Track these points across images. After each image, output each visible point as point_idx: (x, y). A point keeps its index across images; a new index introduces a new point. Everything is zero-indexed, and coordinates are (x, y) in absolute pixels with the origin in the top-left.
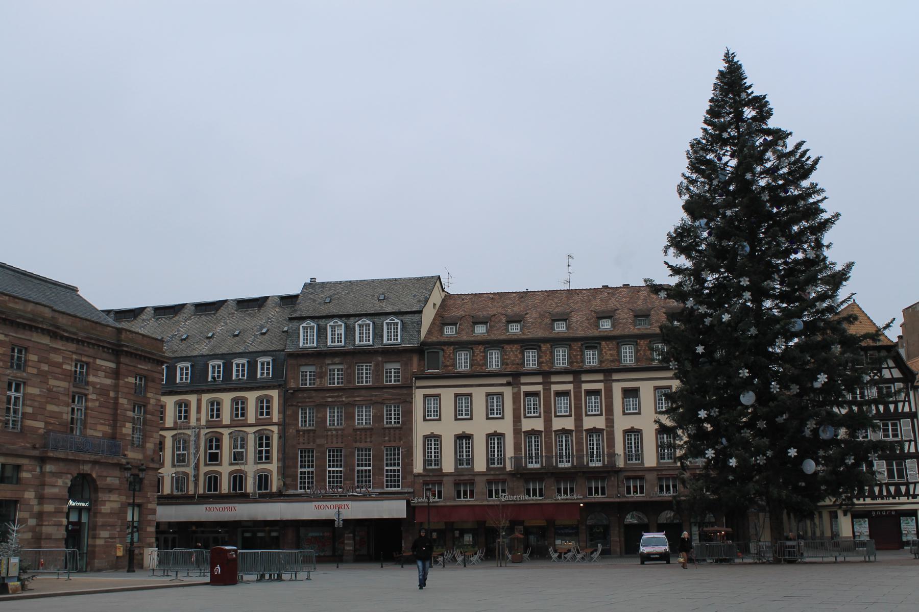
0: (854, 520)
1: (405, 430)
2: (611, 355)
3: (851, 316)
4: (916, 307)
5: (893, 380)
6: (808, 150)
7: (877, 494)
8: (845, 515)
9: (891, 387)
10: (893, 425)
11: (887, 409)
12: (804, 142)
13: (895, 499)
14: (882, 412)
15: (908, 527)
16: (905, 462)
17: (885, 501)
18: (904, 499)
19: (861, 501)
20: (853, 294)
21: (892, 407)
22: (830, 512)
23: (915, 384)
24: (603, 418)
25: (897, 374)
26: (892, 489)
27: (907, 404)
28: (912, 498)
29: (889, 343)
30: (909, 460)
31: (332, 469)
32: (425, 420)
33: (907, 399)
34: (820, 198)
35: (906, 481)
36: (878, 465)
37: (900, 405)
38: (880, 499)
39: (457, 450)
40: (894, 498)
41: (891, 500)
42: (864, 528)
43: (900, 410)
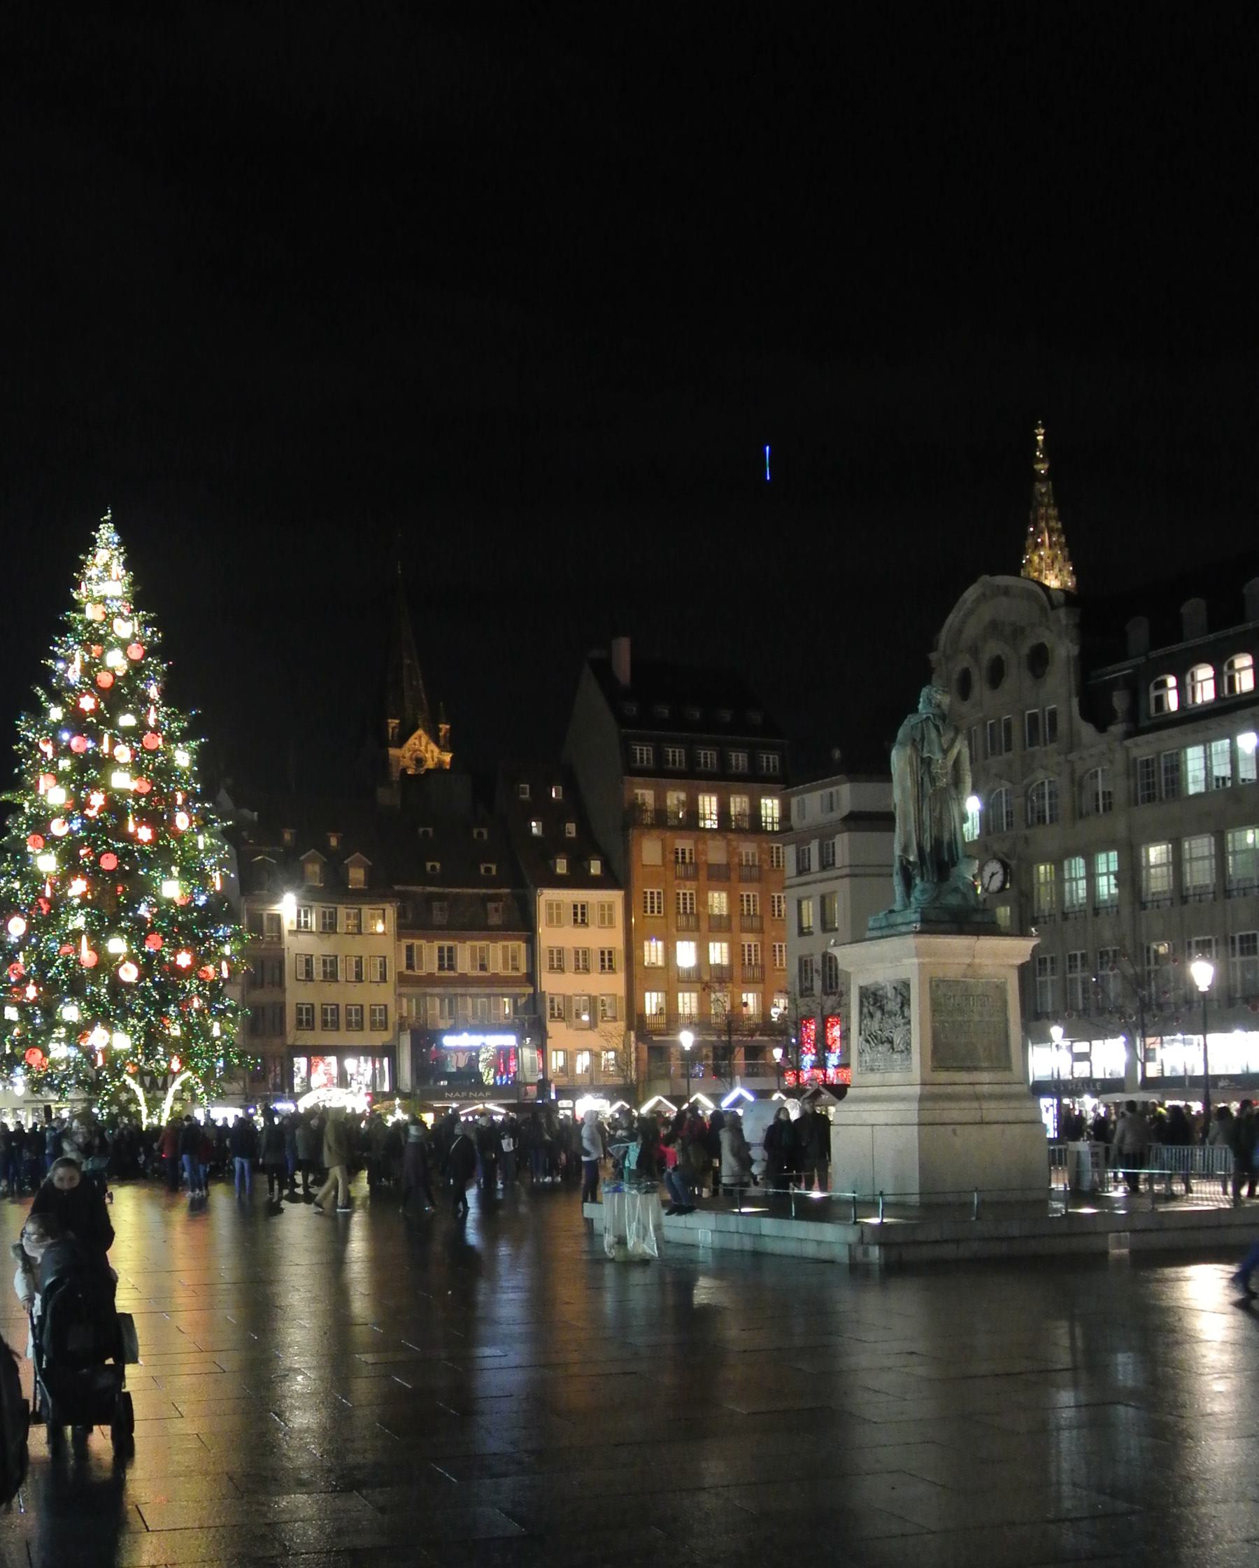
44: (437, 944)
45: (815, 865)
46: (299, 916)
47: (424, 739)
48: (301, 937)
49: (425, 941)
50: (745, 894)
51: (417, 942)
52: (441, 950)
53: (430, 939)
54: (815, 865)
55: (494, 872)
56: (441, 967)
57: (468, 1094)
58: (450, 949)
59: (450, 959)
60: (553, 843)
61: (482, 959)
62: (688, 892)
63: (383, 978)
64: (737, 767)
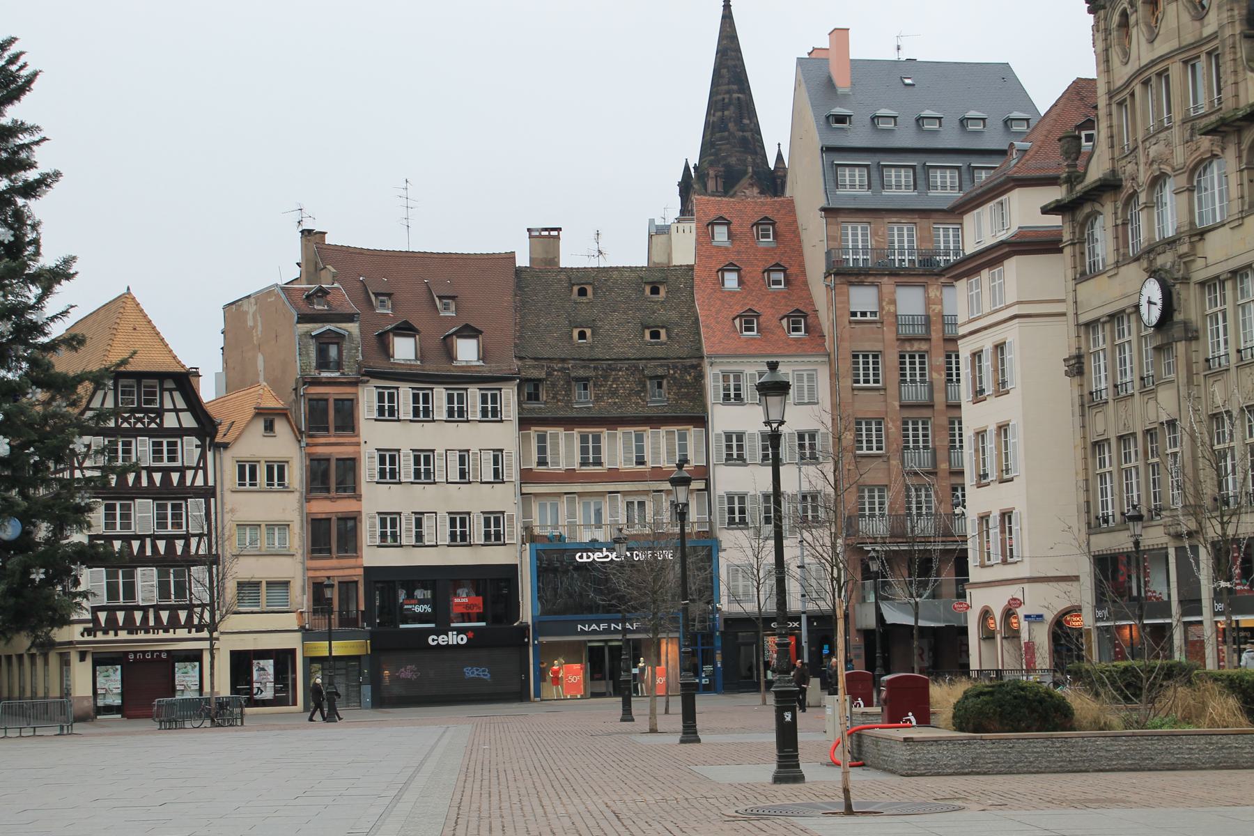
0: (98, 668)
3: (74, 338)
4: (241, 304)
5: (181, 432)
6: (22, 53)
7: (138, 624)
8: (82, 657)
9: (176, 442)
10: (174, 507)
11: (166, 479)
12: (16, 39)
13: (168, 632)
14: (158, 485)
15: (187, 679)
16: (189, 571)
17: (151, 636)
18: (182, 633)
19: (111, 636)
20: (72, 307)
21: (175, 477)
22: (61, 654)
23: (218, 439)
25: (188, 421)
26: (165, 615)
27: (200, 472)
28: (197, 632)
29: (179, 369)
30: (195, 568)
33: (201, 465)
34: (37, 137)
35: (188, 602)
36: (144, 574)
37: (189, 474)
38: (143, 632)
40: (166, 631)
41: (162, 635)
42: (112, 681)
43: (188, 483)
44: (576, 433)
49: (562, 429)
51: (550, 431)
52: (584, 439)
56: (584, 463)
57: (610, 626)
59: (597, 450)
63: (498, 476)
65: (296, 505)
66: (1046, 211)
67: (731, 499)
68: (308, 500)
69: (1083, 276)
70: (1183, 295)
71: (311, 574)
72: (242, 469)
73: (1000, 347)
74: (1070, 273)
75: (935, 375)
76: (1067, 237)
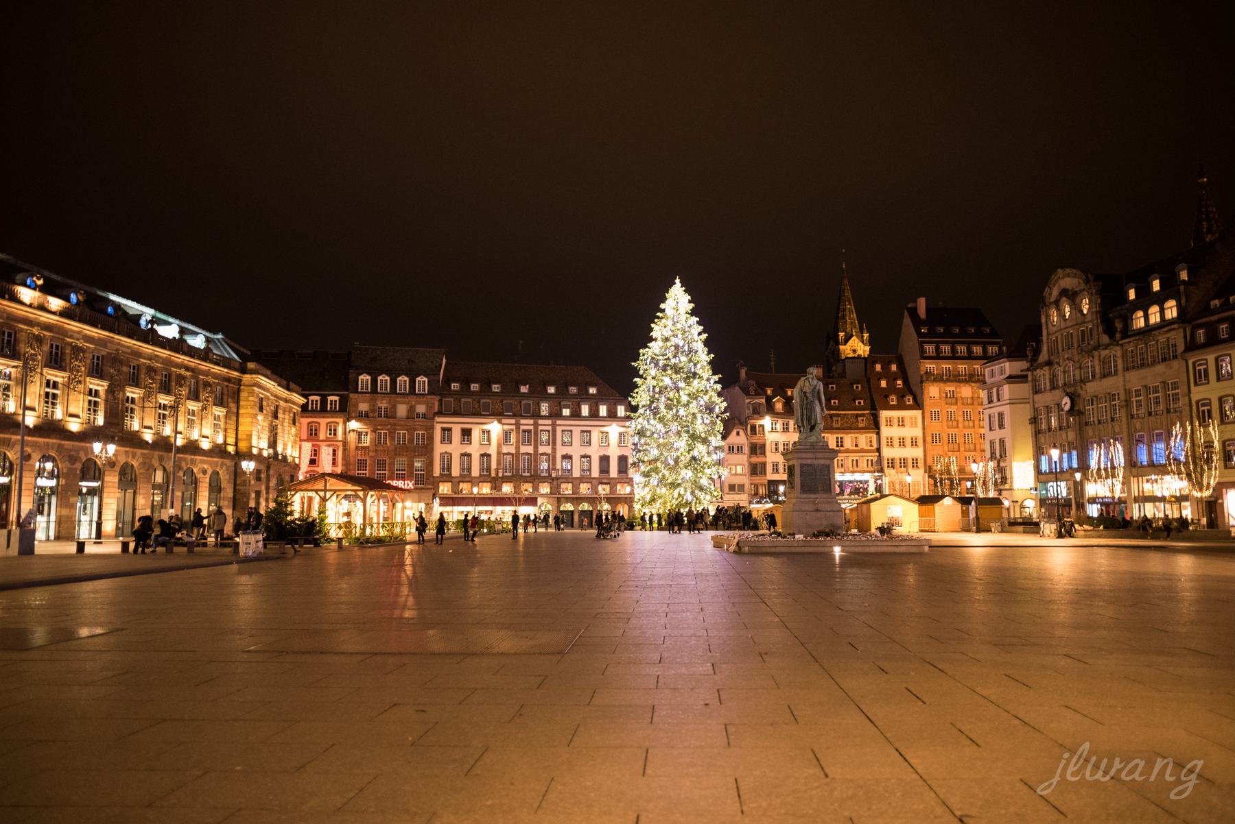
1: (427, 450)
2: (556, 410)
24: (550, 447)
31: (379, 472)
32: (441, 443)
39: (462, 463)
44: (835, 436)
45: (995, 399)
46: (772, 425)
47: (857, 340)
48: (774, 434)
50: (965, 411)
52: (837, 438)
53: (832, 433)
54: (995, 399)
55: (862, 404)
56: (837, 446)
58: (841, 438)
59: (842, 442)
60: (892, 389)
61: (856, 442)
62: (969, 410)
64: (977, 353)
65: (746, 459)
66: (1022, 371)
67: (913, 460)
68: (750, 457)
69: (1036, 391)
70: (1078, 402)
71: (751, 482)
72: (729, 447)
73: (1001, 415)
74: (1031, 391)
75: (959, 418)
76: (1030, 378)
